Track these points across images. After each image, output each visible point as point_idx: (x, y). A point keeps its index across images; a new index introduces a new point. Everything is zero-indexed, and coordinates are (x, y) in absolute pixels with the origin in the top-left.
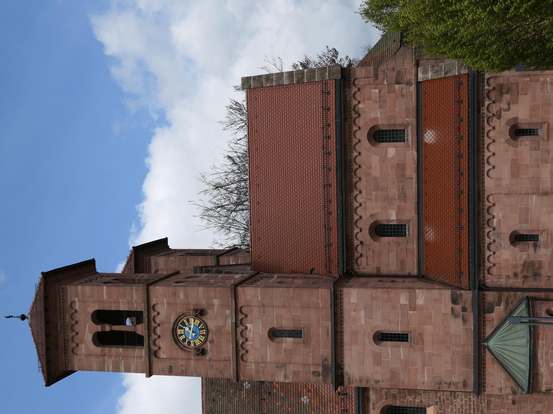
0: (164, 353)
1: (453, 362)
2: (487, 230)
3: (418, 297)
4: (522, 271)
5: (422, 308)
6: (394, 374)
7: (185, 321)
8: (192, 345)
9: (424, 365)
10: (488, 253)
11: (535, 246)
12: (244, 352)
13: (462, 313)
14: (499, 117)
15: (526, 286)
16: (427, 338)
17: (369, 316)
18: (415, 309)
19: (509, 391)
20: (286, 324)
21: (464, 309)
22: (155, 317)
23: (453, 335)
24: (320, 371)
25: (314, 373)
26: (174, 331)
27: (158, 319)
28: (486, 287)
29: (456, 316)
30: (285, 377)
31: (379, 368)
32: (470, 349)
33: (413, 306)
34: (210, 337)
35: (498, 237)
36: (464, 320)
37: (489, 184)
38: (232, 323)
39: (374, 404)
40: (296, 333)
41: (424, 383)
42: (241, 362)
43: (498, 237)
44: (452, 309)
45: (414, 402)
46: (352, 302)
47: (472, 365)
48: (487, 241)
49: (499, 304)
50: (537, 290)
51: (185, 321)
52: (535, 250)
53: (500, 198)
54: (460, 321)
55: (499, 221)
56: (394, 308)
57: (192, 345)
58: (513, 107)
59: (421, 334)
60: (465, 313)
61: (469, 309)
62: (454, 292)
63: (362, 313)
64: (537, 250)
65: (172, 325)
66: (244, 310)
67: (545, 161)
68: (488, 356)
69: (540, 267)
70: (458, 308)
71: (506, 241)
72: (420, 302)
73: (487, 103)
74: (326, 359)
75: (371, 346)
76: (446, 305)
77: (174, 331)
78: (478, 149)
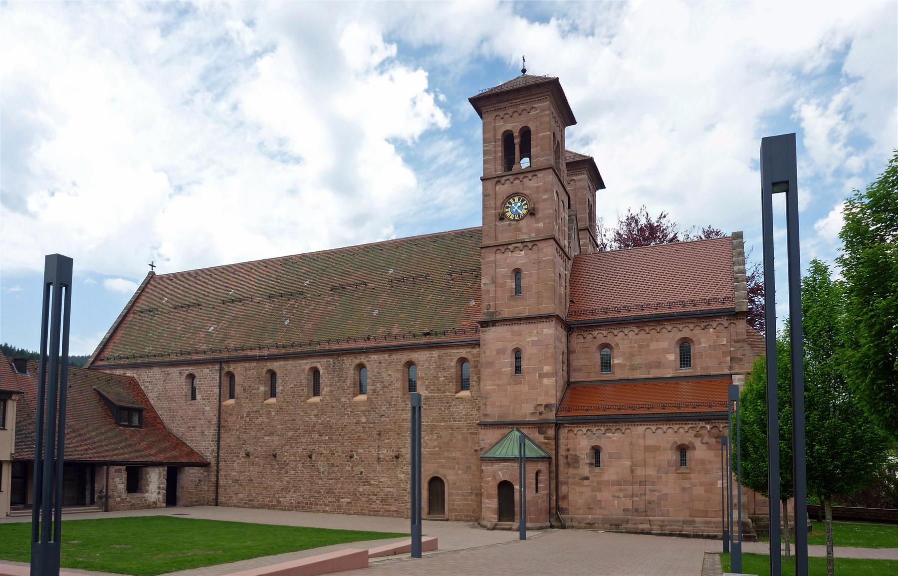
0: (500, 188)
1: (501, 406)
2: (602, 429)
3: (549, 379)
4: (572, 455)
5: (541, 382)
6: (491, 364)
7: (525, 202)
8: (506, 210)
9: (498, 385)
10: (584, 430)
11: (591, 464)
12: (503, 251)
13: (538, 412)
14: (696, 436)
15: (560, 458)
16: (518, 387)
17: (534, 343)
18: (540, 377)
19: (482, 445)
20: (525, 282)
21: (541, 413)
22: (528, 177)
23: (521, 406)
24: (490, 310)
25: (489, 305)
26: (516, 194)
27: (526, 181)
28: (558, 429)
29: (535, 408)
30: (485, 284)
31: (494, 353)
32: (511, 419)
33: (542, 376)
34: (513, 223)
35: (598, 437)
36: (533, 414)
37: (640, 429)
38: (525, 239)
39: (470, 352)
40: (518, 290)
41: (485, 386)
42: (495, 249)
43: (598, 437)
44: (541, 405)
45: (473, 381)
46: (544, 330)
47: (500, 420)
48: (594, 429)
49: (546, 438)
50: (557, 466)
51: (525, 202)
52: (587, 464)
53: (629, 438)
54: (532, 410)
55: (610, 438)
56: (540, 362)
57: (506, 210)
58: (704, 447)
59: (520, 383)
60: (538, 414)
61: (541, 417)
62: (554, 406)
63: (536, 338)
64: (588, 465)
65: (521, 192)
66: (535, 246)
67: (659, 470)
68: (506, 431)
69: (574, 467)
70: (542, 409)
71: (594, 443)
72: (546, 381)
73: (708, 427)
74: (500, 314)
75: (510, 347)
76: (543, 400)
77: (516, 194)
78: (668, 421)
